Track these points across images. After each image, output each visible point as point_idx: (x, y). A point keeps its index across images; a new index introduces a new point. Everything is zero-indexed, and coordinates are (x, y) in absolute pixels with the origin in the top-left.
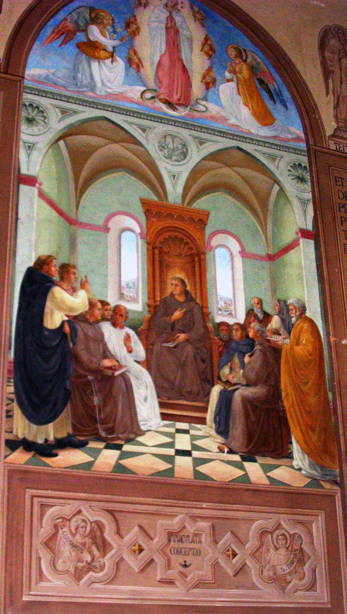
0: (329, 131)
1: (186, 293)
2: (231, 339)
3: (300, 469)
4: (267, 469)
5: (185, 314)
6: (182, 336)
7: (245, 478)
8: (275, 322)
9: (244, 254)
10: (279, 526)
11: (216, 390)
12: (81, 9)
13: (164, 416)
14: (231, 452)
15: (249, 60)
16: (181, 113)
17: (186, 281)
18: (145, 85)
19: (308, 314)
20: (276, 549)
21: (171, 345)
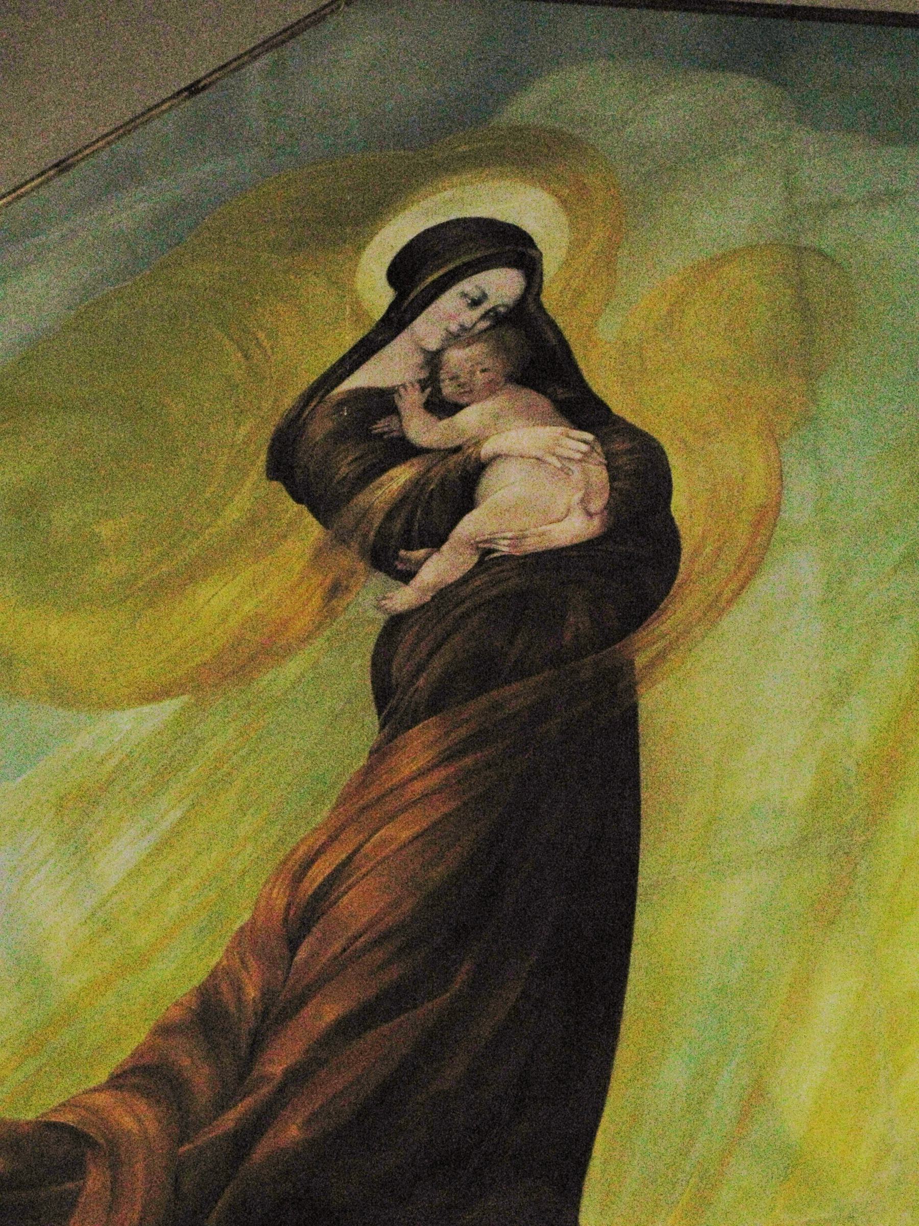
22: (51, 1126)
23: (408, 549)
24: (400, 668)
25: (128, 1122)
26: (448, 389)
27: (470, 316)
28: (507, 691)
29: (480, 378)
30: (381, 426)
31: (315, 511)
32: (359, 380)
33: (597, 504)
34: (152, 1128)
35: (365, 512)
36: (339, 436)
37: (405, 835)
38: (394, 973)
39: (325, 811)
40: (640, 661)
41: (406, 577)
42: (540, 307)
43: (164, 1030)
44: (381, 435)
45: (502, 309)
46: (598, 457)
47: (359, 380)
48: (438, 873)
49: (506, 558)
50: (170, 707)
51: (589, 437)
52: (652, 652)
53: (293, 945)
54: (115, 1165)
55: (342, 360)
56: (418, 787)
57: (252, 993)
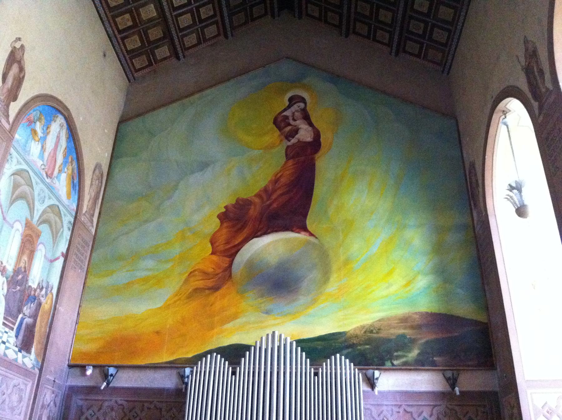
0: (84, 212)
1: (25, 268)
2: (30, 295)
3: (31, 360)
4: (24, 357)
5: (22, 277)
6: (18, 288)
7: (16, 360)
8: (43, 292)
9: (45, 256)
10: (19, 384)
11: (21, 316)
12: (37, 111)
13: (4, 324)
14: (16, 346)
15: (73, 165)
16: (48, 180)
17: (27, 262)
18: (43, 161)
19: (53, 291)
20: (16, 394)
21: (14, 290)
22: (248, 200)
24: (288, 153)
25: (256, 200)
26: (295, 118)
27: (298, 109)
29: (299, 117)
30: (287, 121)
32: (285, 114)
33: (312, 137)
34: (259, 201)
36: (282, 120)
38: (287, 189)
40: (316, 158)
41: (290, 141)
42: (306, 109)
43: (260, 191)
44: (286, 122)
47: (285, 114)
48: (292, 179)
49: (301, 141)
50: (261, 151)
54: (255, 206)
55: (282, 111)
57: (271, 188)
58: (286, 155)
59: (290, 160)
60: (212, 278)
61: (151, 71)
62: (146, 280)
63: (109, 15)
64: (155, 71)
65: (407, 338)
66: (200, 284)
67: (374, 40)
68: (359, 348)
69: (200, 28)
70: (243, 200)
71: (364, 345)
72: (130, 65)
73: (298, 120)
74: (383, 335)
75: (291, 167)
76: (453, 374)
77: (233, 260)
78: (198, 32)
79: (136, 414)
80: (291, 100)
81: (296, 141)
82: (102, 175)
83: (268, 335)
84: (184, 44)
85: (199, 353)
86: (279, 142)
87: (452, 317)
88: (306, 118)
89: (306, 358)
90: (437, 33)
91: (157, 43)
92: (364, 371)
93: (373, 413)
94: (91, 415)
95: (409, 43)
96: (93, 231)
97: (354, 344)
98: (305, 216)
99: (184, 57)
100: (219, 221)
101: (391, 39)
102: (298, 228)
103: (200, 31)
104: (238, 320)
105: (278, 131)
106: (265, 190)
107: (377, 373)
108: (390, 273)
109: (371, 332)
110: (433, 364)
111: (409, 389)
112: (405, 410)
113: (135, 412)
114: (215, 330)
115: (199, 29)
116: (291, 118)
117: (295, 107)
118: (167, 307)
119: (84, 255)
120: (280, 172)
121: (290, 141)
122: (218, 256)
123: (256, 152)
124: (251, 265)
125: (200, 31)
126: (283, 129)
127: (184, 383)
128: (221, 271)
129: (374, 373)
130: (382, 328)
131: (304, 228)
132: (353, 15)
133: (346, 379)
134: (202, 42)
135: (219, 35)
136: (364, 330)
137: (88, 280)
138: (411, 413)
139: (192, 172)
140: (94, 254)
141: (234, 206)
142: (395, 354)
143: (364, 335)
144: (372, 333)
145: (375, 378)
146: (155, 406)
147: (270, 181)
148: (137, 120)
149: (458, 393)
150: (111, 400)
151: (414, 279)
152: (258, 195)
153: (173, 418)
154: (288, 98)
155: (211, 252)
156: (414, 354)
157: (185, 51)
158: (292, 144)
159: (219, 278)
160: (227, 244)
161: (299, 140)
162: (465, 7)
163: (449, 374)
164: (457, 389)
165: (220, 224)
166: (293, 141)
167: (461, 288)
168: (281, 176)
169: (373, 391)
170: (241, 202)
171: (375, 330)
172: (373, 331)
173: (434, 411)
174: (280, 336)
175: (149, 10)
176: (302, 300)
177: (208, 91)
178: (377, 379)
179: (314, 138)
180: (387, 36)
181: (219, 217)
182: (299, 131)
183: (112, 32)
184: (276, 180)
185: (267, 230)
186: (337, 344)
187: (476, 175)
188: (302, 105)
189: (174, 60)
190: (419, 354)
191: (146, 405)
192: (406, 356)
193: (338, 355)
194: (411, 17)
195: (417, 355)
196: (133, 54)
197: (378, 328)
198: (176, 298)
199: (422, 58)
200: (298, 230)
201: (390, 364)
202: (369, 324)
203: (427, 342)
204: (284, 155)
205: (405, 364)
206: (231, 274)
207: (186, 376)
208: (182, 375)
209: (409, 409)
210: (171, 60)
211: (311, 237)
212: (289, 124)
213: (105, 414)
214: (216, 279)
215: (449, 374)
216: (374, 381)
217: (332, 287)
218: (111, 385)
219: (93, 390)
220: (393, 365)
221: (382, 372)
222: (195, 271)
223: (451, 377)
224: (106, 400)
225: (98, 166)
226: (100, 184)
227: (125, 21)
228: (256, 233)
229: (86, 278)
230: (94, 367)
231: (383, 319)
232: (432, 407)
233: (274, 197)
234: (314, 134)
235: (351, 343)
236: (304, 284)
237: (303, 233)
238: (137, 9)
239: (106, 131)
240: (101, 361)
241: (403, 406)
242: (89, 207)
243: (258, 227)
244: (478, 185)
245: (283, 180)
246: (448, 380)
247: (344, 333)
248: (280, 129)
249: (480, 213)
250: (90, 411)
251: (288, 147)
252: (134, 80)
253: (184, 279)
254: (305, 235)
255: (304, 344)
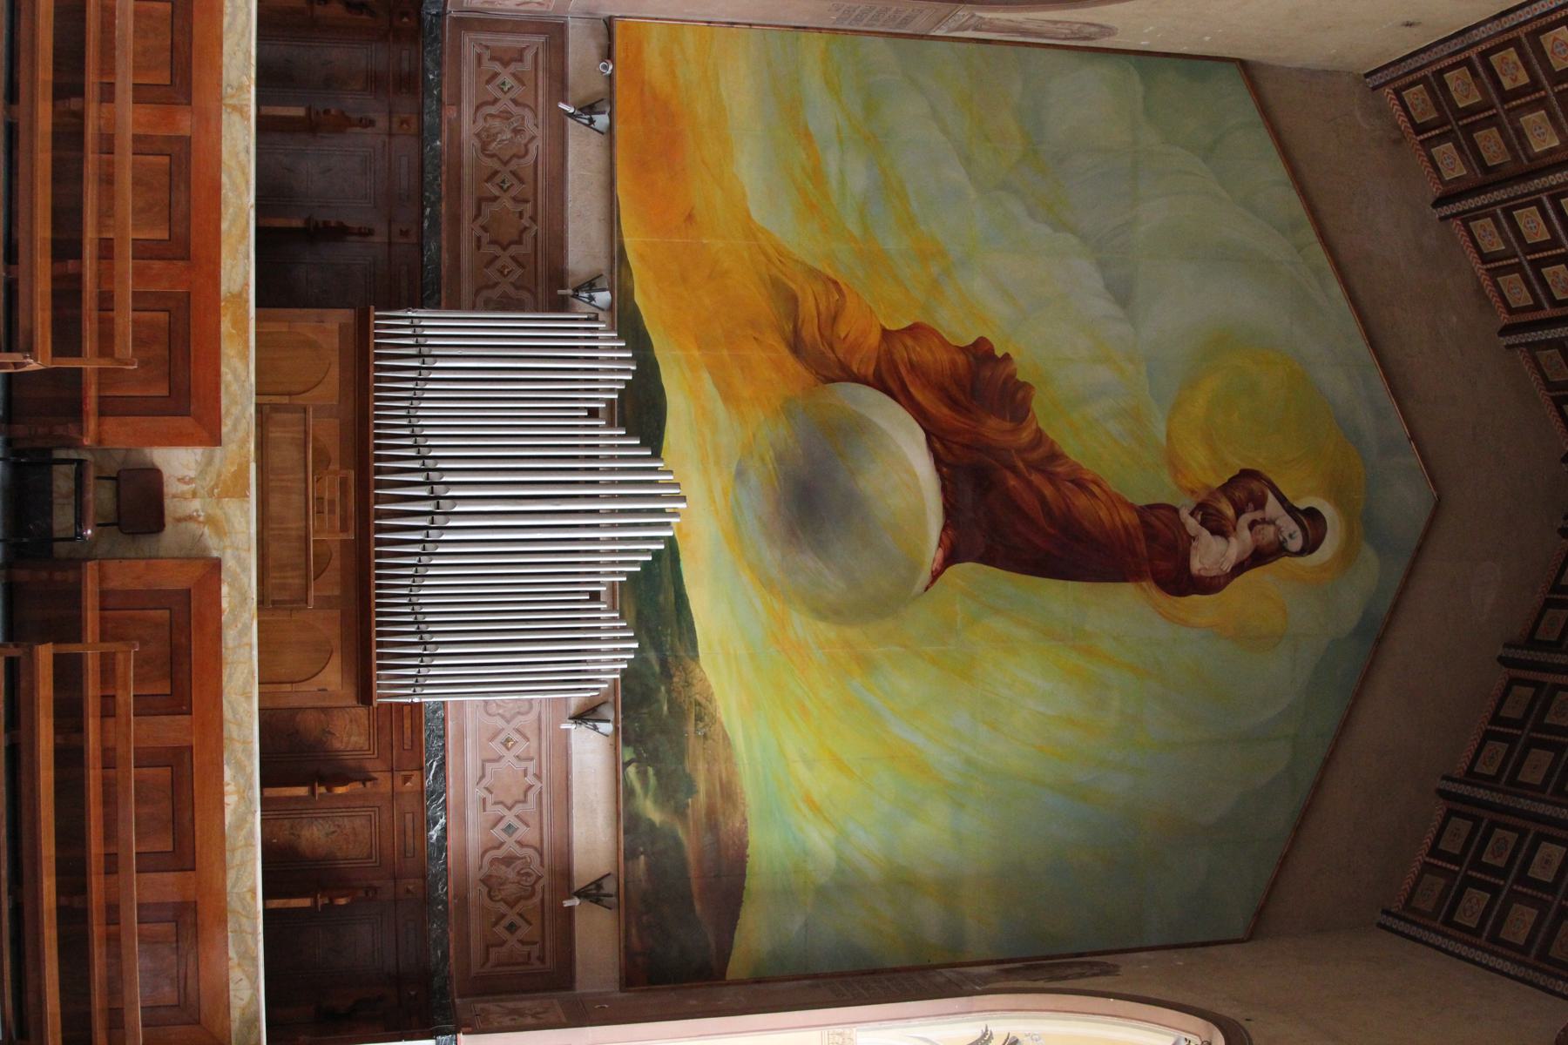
0: (978, 14)
22: (1029, 411)
23: (1202, 515)
25: (1024, 435)
26: (1259, 527)
28: (1143, 545)
29: (1260, 537)
31: (1224, 485)
32: (1271, 497)
33: (1203, 573)
35: (1220, 501)
37: (1101, 514)
39: (1114, 489)
40: (1144, 584)
41: (1192, 514)
43: (1052, 443)
45: (1285, 544)
46: (1220, 573)
49: (1191, 544)
50: (1164, 441)
51: (1229, 570)
52: (1147, 588)
53: (1072, 481)
55: (1281, 493)
56: (1117, 519)
57: (1059, 469)
58: (1151, 507)
59: (1141, 516)
60: (822, 335)
61: (1400, 130)
62: (817, 174)
63: (1521, 32)
64: (1397, 142)
65: (688, 798)
66: (808, 307)
67: (1488, 736)
68: (663, 688)
69: (1520, 263)
70: (1027, 400)
71: (669, 701)
72: (1410, 79)
73: (1252, 536)
74: (693, 745)
75: (1119, 524)
76: (611, 896)
77: (868, 384)
78: (1509, 258)
79: (508, 187)
80: (1313, 514)
81: (1192, 535)
82: (1085, 38)
83: (677, 485)
84: (1476, 218)
85: (644, 318)
86: (1189, 485)
87: (739, 902)
88: (1259, 557)
89: (629, 574)
90: (1478, 901)
91: (1472, 153)
92: (611, 699)
93: (521, 718)
94: (504, 83)
95: (1465, 826)
96: (939, 33)
97: (670, 677)
98: (988, 559)
99: (1442, 219)
100: (971, 343)
101: (1489, 781)
102: (952, 543)
103: (1513, 261)
104: (720, 404)
105: (1220, 484)
106: (1055, 456)
107: (607, 728)
108: (839, 764)
109: (699, 718)
110: (630, 854)
111: (575, 799)
112: (530, 787)
113: (512, 185)
114: (696, 353)
115: (1517, 260)
116: (1258, 515)
117: (1288, 525)
118: (751, 231)
119: (874, 22)
120: (1104, 491)
121: (1192, 514)
122: (879, 346)
123: (1160, 429)
124: (854, 430)
125: (1513, 261)
126: (1225, 495)
127: (577, 290)
128: (841, 356)
129: (608, 721)
130: (710, 741)
131: (952, 555)
132: (1550, 679)
133: (585, 661)
134: (1489, 266)
135: (1511, 311)
136: (703, 702)
137: (816, 34)
138: (525, 801)
139: (1102, 265)
140: (880, 41)
141: (1012, 376)
142: (651, 771)
143: (691, 703)
144: (696, 720)
145: (596, 724)
146: (525, 228)
147: (1077, 467)
148: (1251, 105)
149: (567, 903)
150: (536, 126)
151: (826, 819)
152: (1040, 438)
153: (502, 273)
154: (1319, 508)
155: (887, 327)
156: (652, 811)
157: (1461, 220)
158: (1183, 521)
159: (823, 353)
160: (908, 365)
161: (1194, 538)
162: (1520, 971)
163: (610, 887)
164: (576, 902)
165: (963, 345)
166: (1192, 524)
167: (806, 925)
168: (1094, 495)
169: (570, 719)
170: (1020, 395)
171: (704, 727)
172: (701, 721)
173: (530, 852)
174: (675, 514)
175: (1544, 134)
176: (770, 556)
177: (1336, 290)
178: (595, 728)
179: (1201, 579)
180: (1491, 770)
181: (981, 342)
182: (1224, 539)
183: (1478, 38)
184: (1080, 484)
185: (947, 465)
186: (669, 638)
187: (1081, 976)
188: (1296, 544)
189: (1435, 190)
190: (652, 824)
191: (528, 207)
192: (646, 794)
193: (636, 645)
194: (1523, 833)
195: (649, 819)
196: (1437, 86)
197: (709, 734)
198: (771, 251)
199: (1427, 859)
200: (947, 542)
201: (627, 759)
202: (718, 715)
203: (678, 843)
204: (1151, 501)
205: (630, 793)
206: (833, 381)
207: (592, 294)
208: (594, 285)
209: (532, 796)
210: (1434, 183)
211: (930, 574)
212: (1239, 512)
213: (506, 116)
214: (821, 347)
215: (610, 887)
216: (588, 720)
217: (802, 626)
218: (569, 119)
219: (560, 85)
220: (626, 765)
221: (610, 740)
222: (840, 290)
223: (603, 892)
224: (536, 116)
225: (1106, 31)
226: (1063, 36)
227: (1513, 73)
228: (941, 439)
229: (819, 30)
230: (611, 77)
231: (729, 744)
232: (538, 845)
233: (1035, 478)
234: (1211, 578)
235: (672, 672)
236: (809, 561)
237: (940, 555)
238: (1541, 103)
239: (1207, 38)
240: (624, 97)
241: (540, 785)
242: (997, 22)
243: (957, 443)
244: (1051, 979)
245: (1081, 501)
246: (598, 884)
247: (695, 657)
248: (1226, 488)
249: (985, 979)
250: (510, 81)
251: (1175, 510)
252: (1371, 86)
253: (819, 266)
254: (934, 560)
255: (666, 563)
